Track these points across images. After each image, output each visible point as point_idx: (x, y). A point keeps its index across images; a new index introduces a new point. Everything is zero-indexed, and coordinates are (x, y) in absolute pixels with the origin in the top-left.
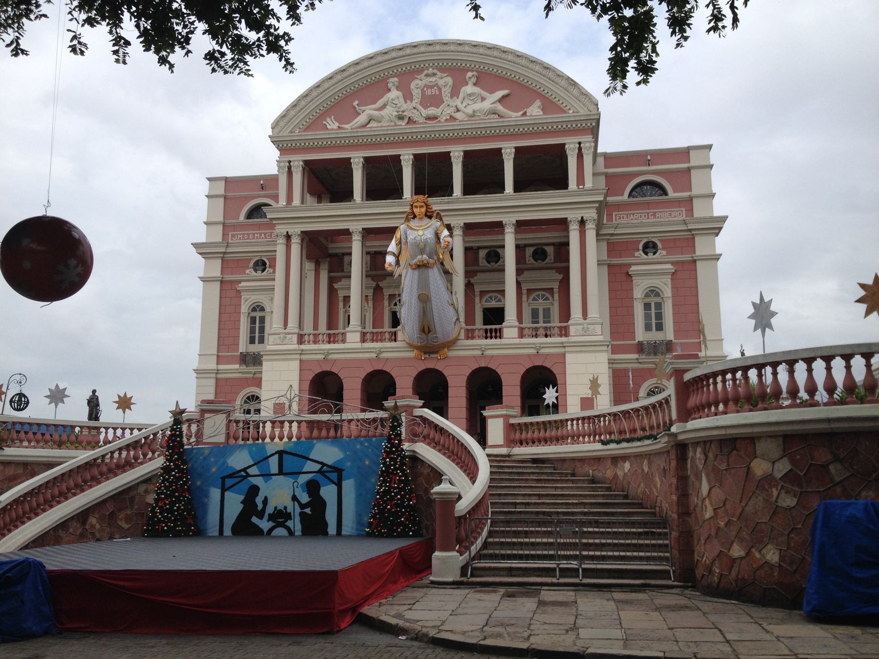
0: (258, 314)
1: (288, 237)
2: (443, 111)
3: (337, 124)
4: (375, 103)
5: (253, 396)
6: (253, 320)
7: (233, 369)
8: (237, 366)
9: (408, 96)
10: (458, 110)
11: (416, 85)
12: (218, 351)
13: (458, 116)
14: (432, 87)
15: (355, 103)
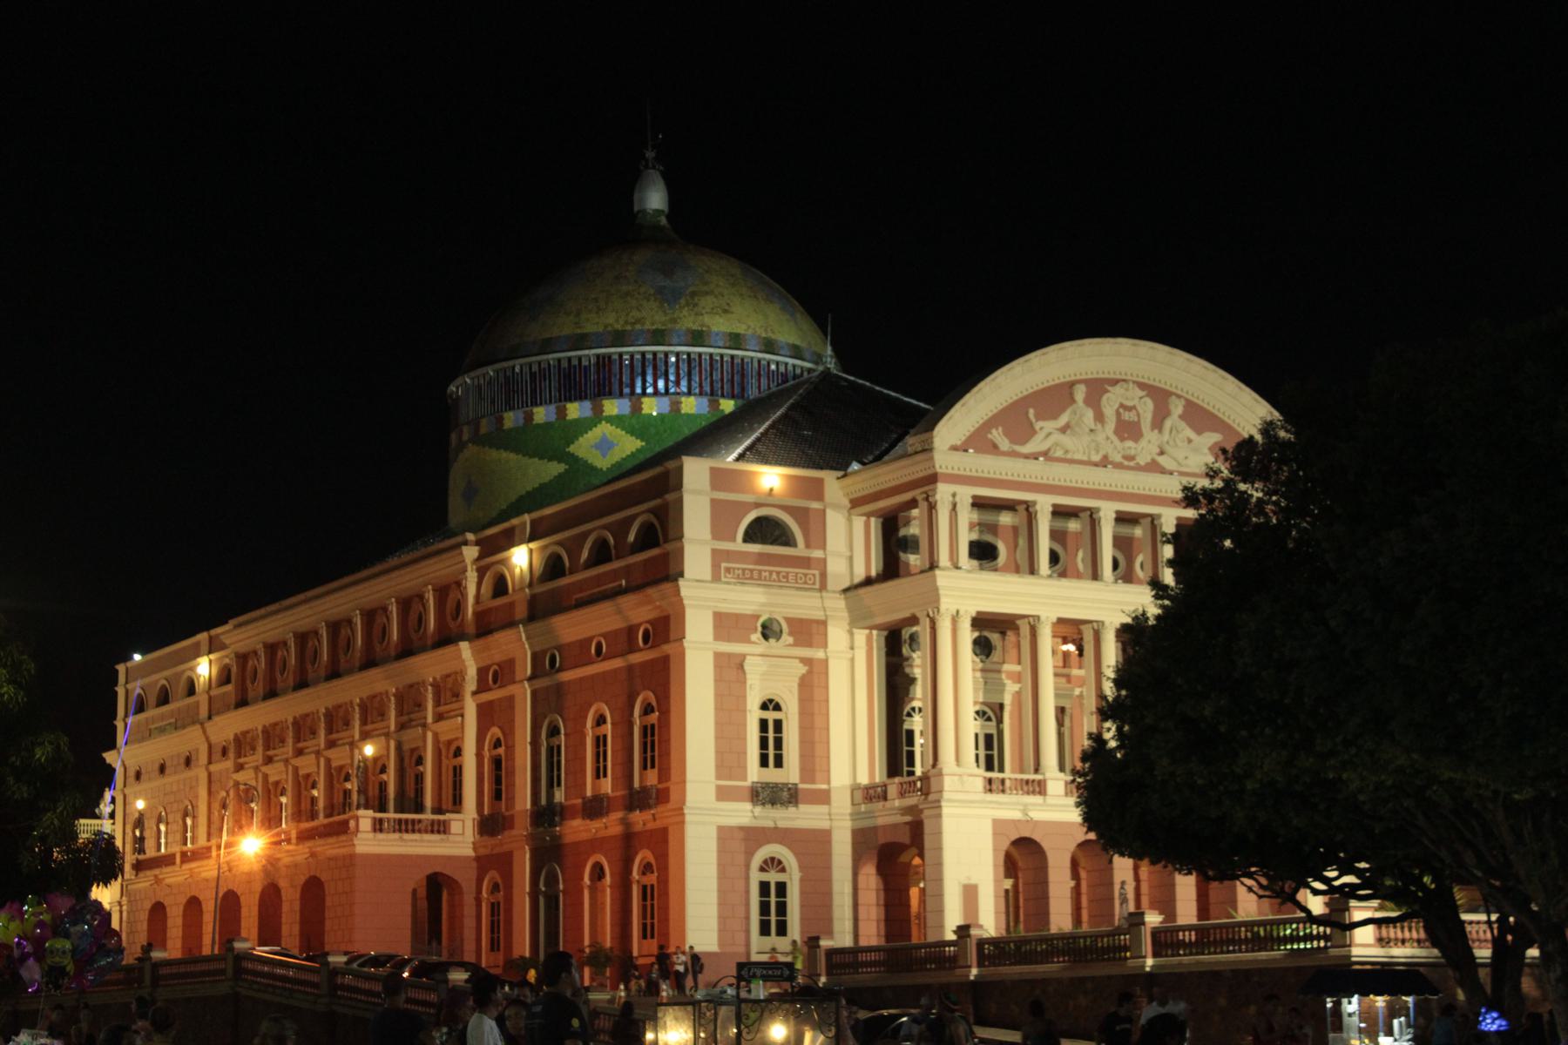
0: (771, 716)
1: (955, 619)
2: (1145, 449)
3: (1004, 444)
4: (1055, 417)
5: (773, 859)
6: (763, 724)
7: (743, 814)
8: (748, 806)
9: (1100, 417)
10: (1162, 453)
11: (1111, 402)
12: (719, 777)
13: (1162, 460)
14: (1129, 409)
15: (1031, 412)
